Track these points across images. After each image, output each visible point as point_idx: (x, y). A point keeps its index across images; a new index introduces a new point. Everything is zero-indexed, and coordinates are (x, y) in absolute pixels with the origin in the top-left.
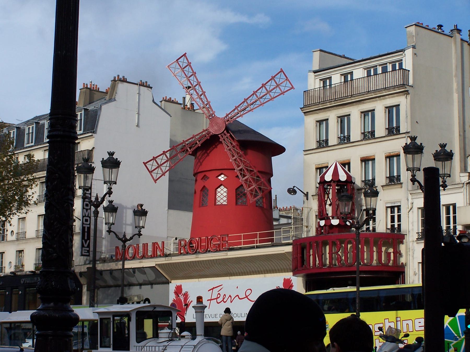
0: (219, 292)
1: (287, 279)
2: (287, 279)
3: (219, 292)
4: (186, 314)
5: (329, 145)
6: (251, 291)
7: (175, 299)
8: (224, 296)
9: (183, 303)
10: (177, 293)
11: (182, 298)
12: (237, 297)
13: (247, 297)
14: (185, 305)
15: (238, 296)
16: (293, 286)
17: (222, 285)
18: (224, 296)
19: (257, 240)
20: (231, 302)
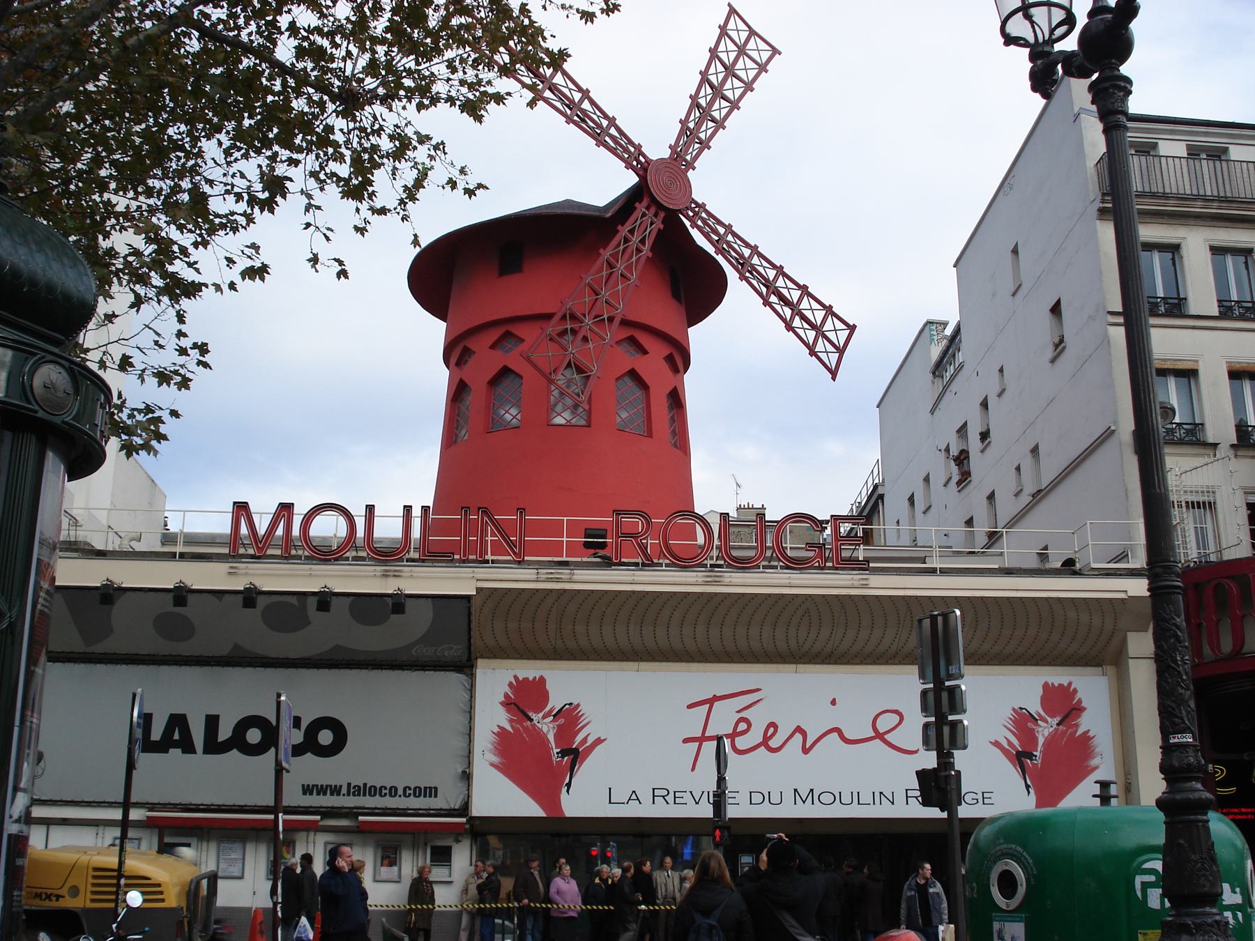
0: (744, 714)
1: (1056, 685)
2: (1056, 685)
3: (744, 714)
4: (569, 785)
5: (1192, 312)
6: (897, 718)
8: (771, 730)
9: (554, 747)
10: (519, 708)
11: (548, 728)
12: (836, 734)
14: (563, 753)
15: (837, 730)
16: (1084, 709)
17: (758, 690)
18: (771, 730)
20: (806, 751)
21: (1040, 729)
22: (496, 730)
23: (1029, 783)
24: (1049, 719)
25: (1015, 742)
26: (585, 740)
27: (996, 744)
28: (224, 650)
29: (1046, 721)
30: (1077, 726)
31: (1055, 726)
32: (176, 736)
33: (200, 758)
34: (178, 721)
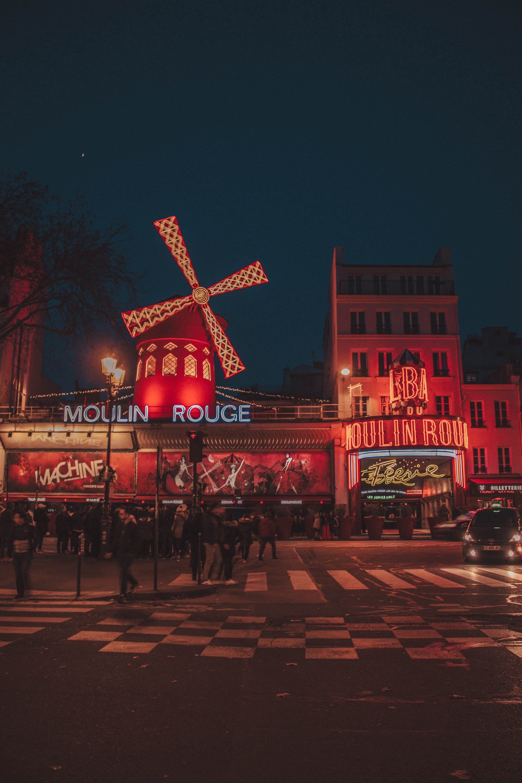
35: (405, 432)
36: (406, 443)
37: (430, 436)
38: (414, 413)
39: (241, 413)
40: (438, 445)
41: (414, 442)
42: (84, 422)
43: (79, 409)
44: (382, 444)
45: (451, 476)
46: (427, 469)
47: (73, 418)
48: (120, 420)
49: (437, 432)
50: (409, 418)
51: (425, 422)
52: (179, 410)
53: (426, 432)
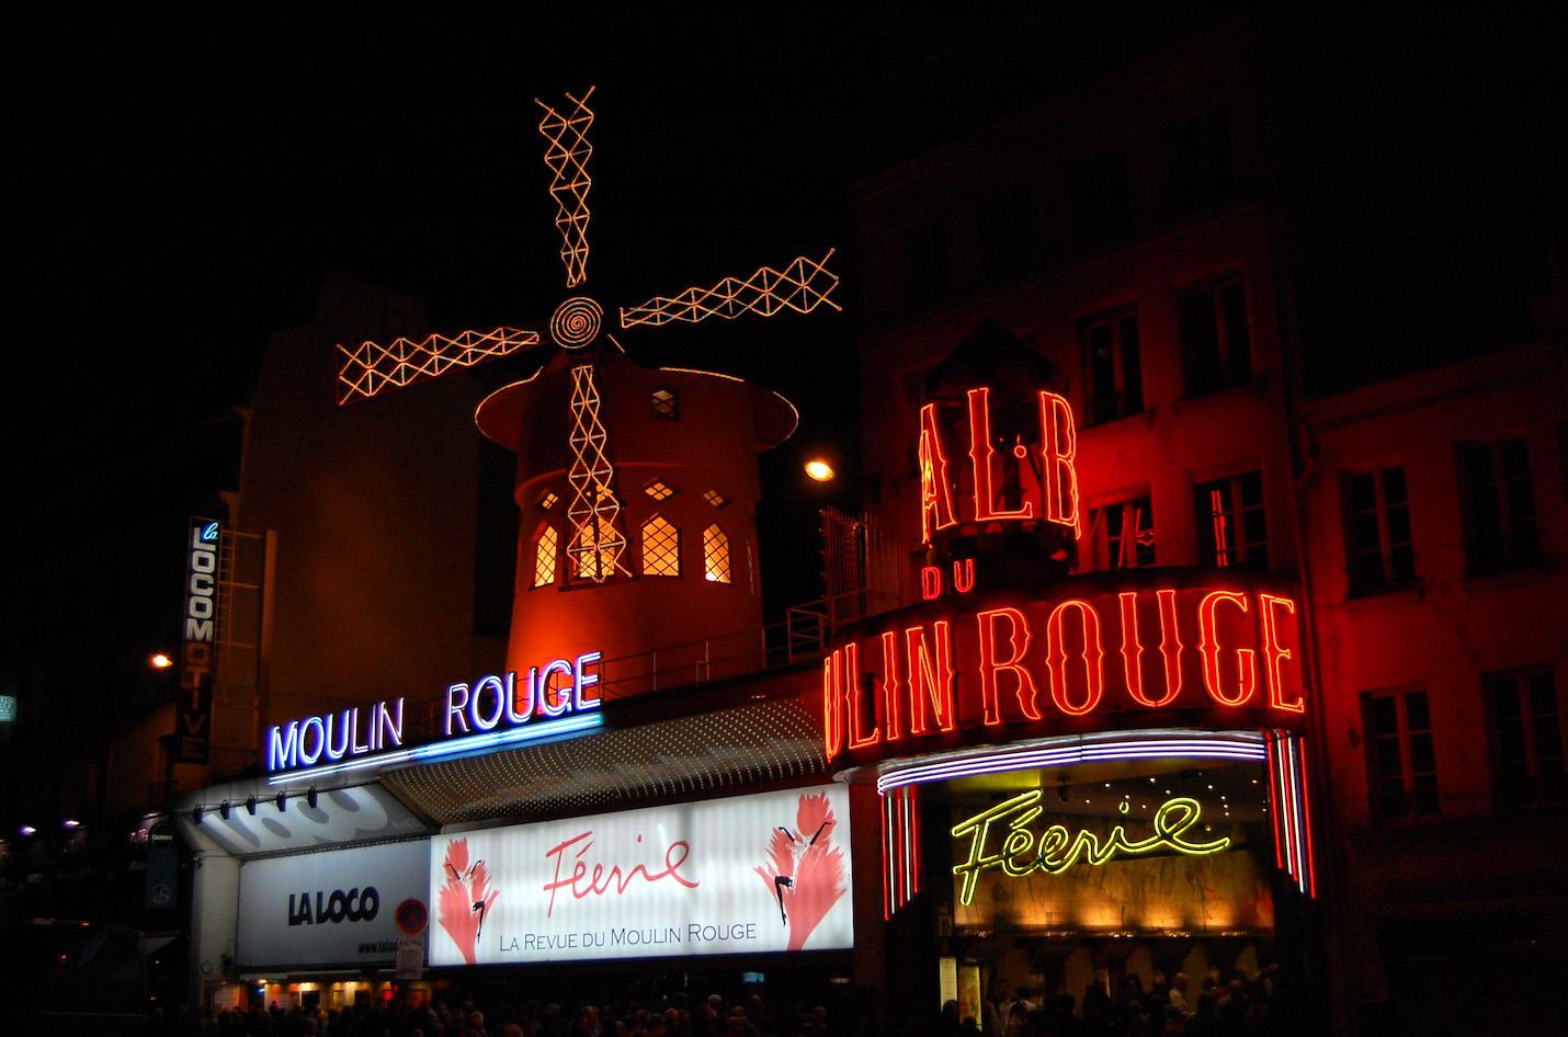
0: (580, 859)
2: (811, 797)
3: (580, 859)
7: (448, 888)
12: (640, 872)
13: (671, 870)
17: (590, 833)
19: (703, 666)
20: (620, 891)
21: (796, 850)
22: (441, 890)
23: (785, 912)
24: (804, 837)
25: (775, 866)
26: (487, 896)
27: (760, 871)
28: (313, 842)
29: (801, 841)
30: (827, 843)
31: (809, 845)
32: (305, 912)
33: (315, 926)
34: (305, 898)
35: (916, 680)
36: (918, 726)
37: (1008, 679)
38: (944, 592)
39: (582, 680)
40: (1039, 718)
41: (944, 718)
42: (301, 766)
43: (292, 730)
44: (854, 743)
45: (1259, 842)
46: (1159, 821)
47: (283, 758)
48: (356, 750)
49: (1034, 661)
50: (924, 613)
51: (987, 617)
52: (458, 697)
53: (989, 669)
